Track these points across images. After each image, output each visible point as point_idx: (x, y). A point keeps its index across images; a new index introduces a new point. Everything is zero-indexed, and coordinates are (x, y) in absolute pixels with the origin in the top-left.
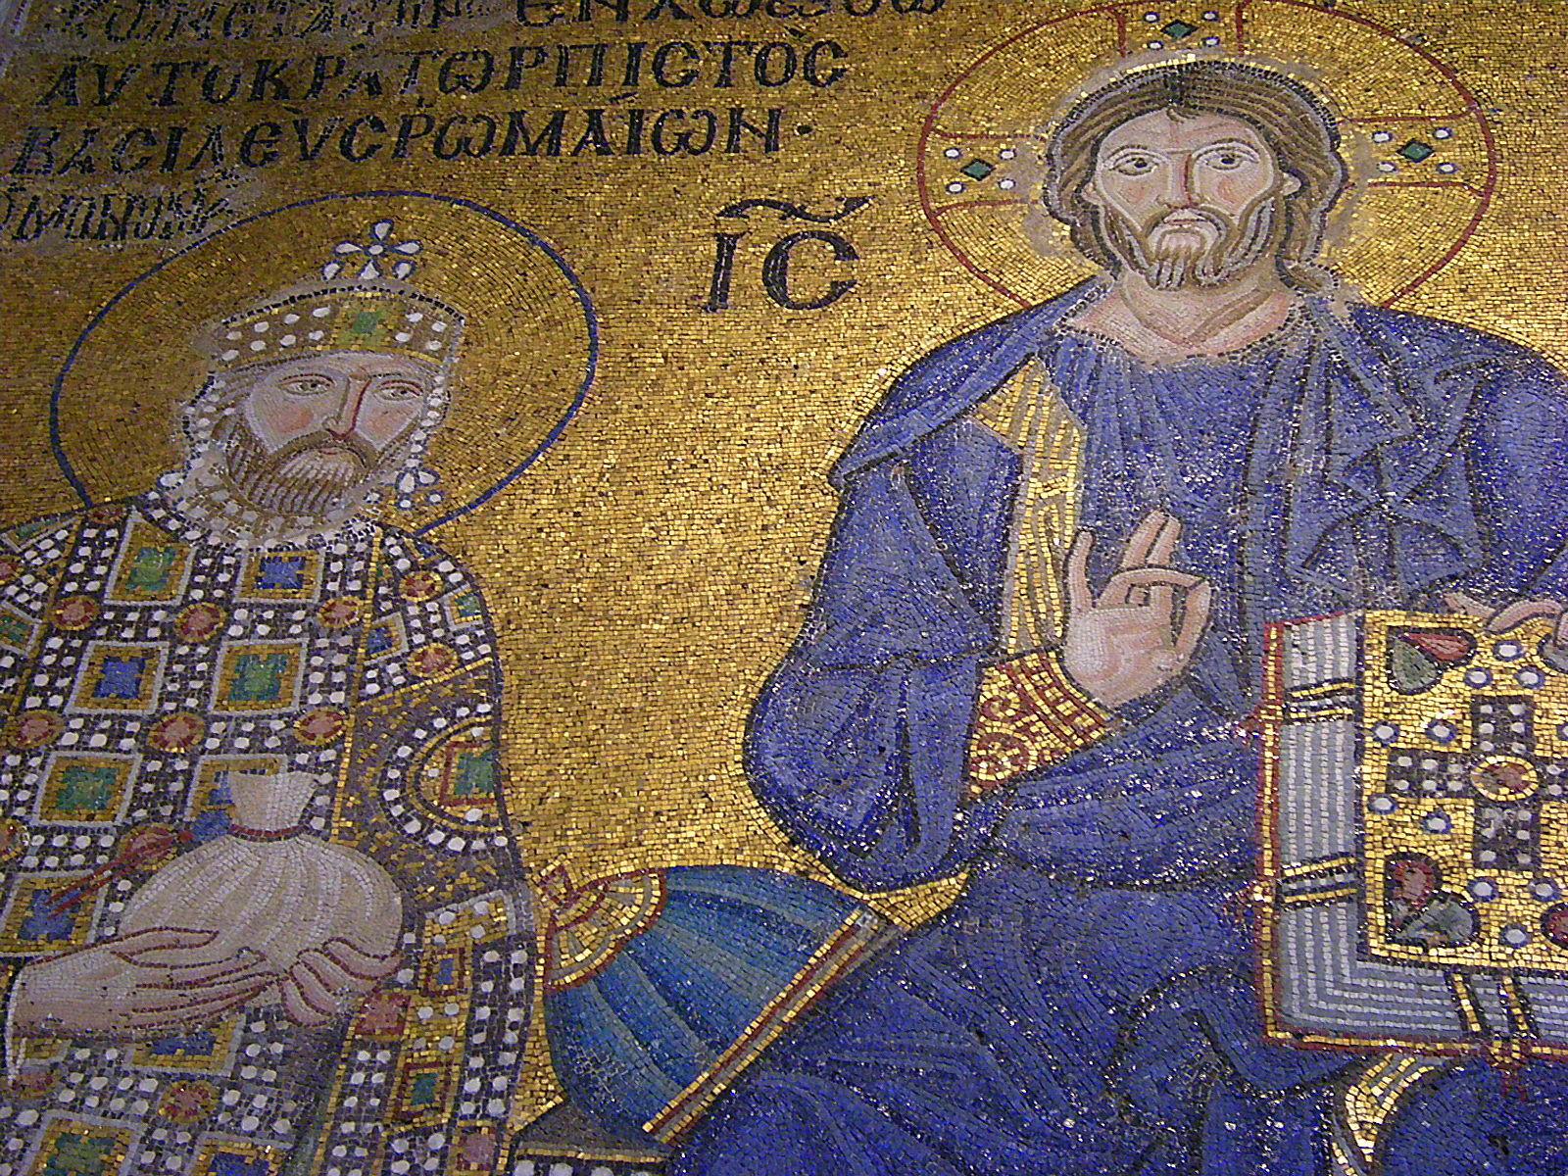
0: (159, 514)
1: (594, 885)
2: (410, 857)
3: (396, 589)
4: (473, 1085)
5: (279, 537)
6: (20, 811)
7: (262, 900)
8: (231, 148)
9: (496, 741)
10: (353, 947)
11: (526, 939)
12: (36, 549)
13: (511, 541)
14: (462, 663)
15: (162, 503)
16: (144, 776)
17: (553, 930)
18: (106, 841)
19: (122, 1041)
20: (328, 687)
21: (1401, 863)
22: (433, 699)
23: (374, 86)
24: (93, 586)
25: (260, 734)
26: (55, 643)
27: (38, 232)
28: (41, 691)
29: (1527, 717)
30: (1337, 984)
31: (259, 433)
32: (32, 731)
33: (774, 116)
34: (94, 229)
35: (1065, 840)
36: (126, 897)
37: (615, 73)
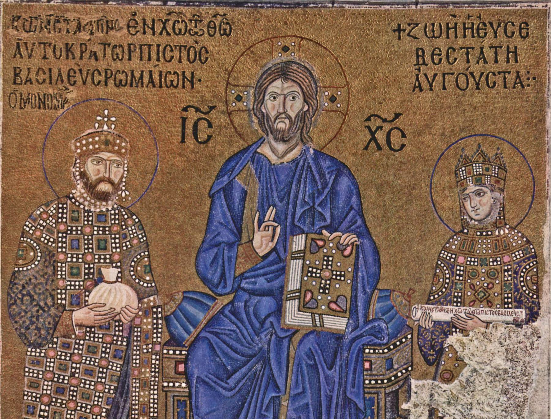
5: (100, 208)
6: (64, 276)
8: (65, 78)
15: (73, 198)
16: (85, 269)
19: (94, 327)
20: (116, 248)
23: (96, 59)
24: (64, 220)
25: (105, 259)
26: (60, 235)
27: (25, 106)
28: (62, 247)
30: (294, 316)
36: (88, 296)
37: (154, 56)
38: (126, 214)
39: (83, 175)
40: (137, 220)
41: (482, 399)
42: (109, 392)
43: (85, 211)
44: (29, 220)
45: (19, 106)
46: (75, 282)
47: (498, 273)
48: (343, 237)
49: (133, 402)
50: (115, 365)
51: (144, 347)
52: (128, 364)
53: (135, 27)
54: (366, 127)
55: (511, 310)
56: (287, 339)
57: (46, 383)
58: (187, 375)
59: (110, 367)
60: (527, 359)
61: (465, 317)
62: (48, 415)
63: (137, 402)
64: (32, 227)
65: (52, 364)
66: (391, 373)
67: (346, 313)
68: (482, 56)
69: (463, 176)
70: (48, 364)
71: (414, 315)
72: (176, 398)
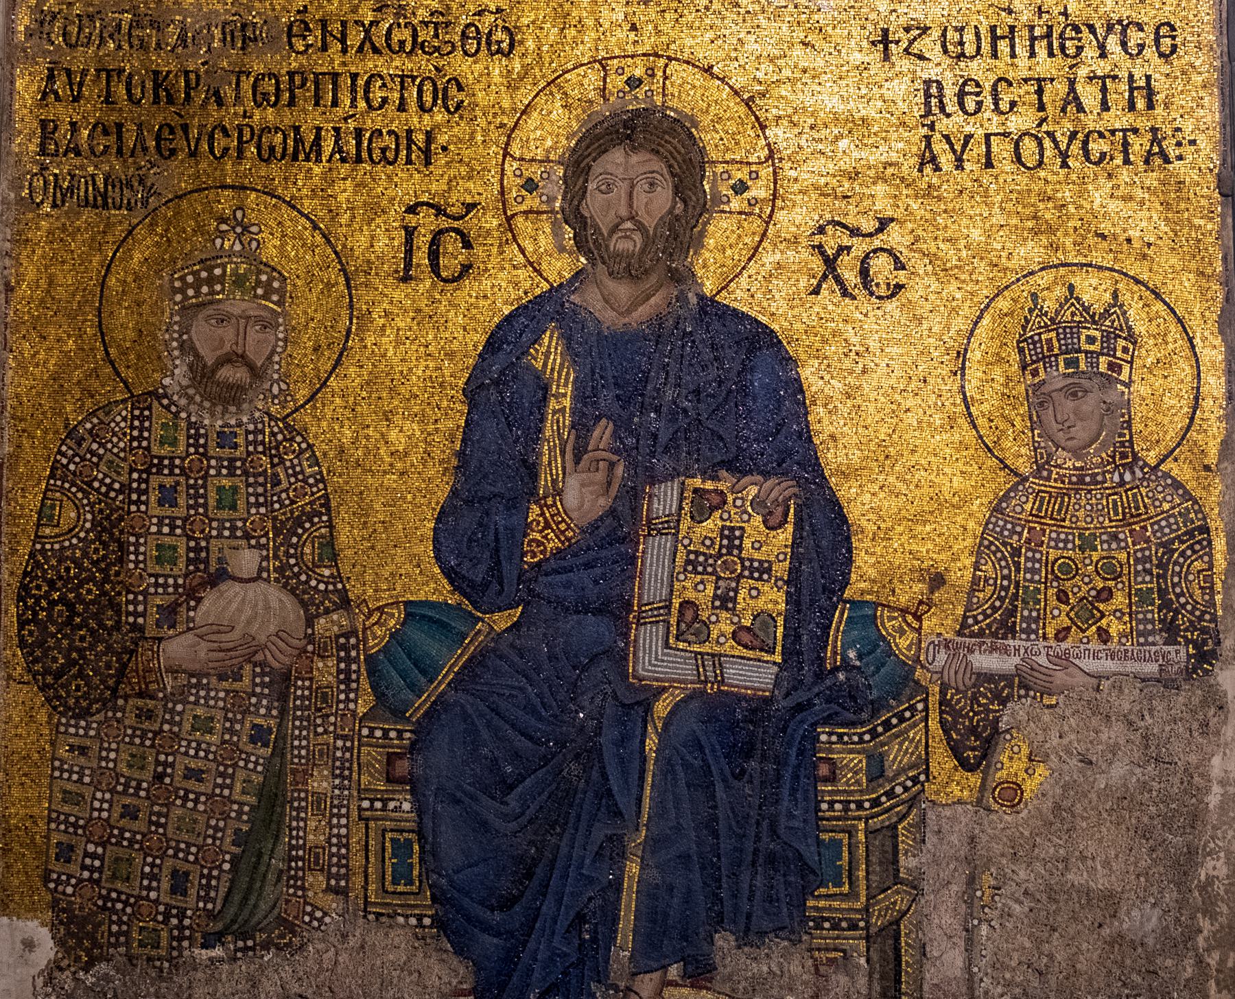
0: (165, 402)
1: (378, 609)
2: (304, 592)
4: (342, 697)
5: (222, 418)
6: (141, 566)
9: (331, 535)
11: (354, 632)
13: (324, 424)
14: (313, 494)
15: (165, 396)
16: (189, 549)
17: (365, 630)
18: (180, 581)
19: (207, 675)
20: (258, 505)
21: (686, 604)
23: (220, 102)
24: (145, 444)
25: (233, 529)
26: (135, 475)
29: (741, 538)
30: (656, 659)
31: (202, 352)
32: (137, 524)
33: (429, 137)
34: (91, 198)
35: (561, 592)
36: (195, 609)
38: (281, 432)
39: (187, 348)
40: (304, 446)
41: (1091, 850)
42: (238, 818)
43: (190, 425)
46: (166, 577)
47: (1121, 567)
48: (769, 483)
49: (294, 842)
50: (253, 758)
51: (319, 721)
52: (283, 755)
53: (304, 37)
54: (813, 247)
55: (1154, 649)
56: (641, 710)
57: (99, 795)
58: (414, 785)
59: (242, 763)
60: (1193, 759)
61: (1047, 664)
62: (102, 865)
63: (301, 842)
64: (74, 456)
65: (112, 755)
66: (880, 786)
67: (774, 653)
68: (1073, 99)
69: (1036, 354)
71: (930, 659)
72: (389, 835)
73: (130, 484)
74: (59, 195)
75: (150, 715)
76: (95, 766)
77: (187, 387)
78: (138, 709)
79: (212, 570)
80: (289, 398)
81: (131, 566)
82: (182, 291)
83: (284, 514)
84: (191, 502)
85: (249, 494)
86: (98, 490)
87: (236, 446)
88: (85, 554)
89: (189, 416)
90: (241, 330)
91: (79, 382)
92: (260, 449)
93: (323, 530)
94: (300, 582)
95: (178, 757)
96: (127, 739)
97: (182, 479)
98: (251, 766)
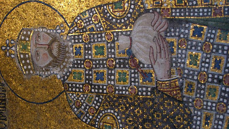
0: (66, 77)
2: (135, 14)
3: (81, 29)
6: (127, 88)
7: (144, 40)
9: (112, 3)
10: (153, 21)
12: (74, 99)
14: (96, 13)
15: (64, 77)
16: (120, 67)
18: (133, 71)
19: (171, 58)
20: (101, 37)
22: (103, 17)
24: (81, 86)
25: (111, 48)
26: (93, 90)
28: (103, 90)
31: (49, 62)
36: (143, 65)
38: (74, 28)
40: (79, 18)
44: (81, 118)
45: (4, 121)
46: (131, 77)
50: (209, 35)
52: (207, 20)
59: (212, 41)
64: (87, 116)
70: (209, 108)
73: (96, 93)
74: (2, 118)
75: (190, 85)
76: (215, 113)
77: (61, 68)
78: (187, 91)
79: (127, 57)
80: (62, 25)
81: (127, 93)
82: (29, 70)
83: (104, 25)
84: (102, 66)
85: (98, 41)
86: (99, 107)
87: (80, 47)
88: (124, 113)
89: (70, 67)
90: (40, 46)
91: (61, 113)
92: (80, 37)
93: (110, 8)
94: (131, 17)
95: (210, 71)
96: (202, 97)
97: (93, 70)
98: (212, 36)
